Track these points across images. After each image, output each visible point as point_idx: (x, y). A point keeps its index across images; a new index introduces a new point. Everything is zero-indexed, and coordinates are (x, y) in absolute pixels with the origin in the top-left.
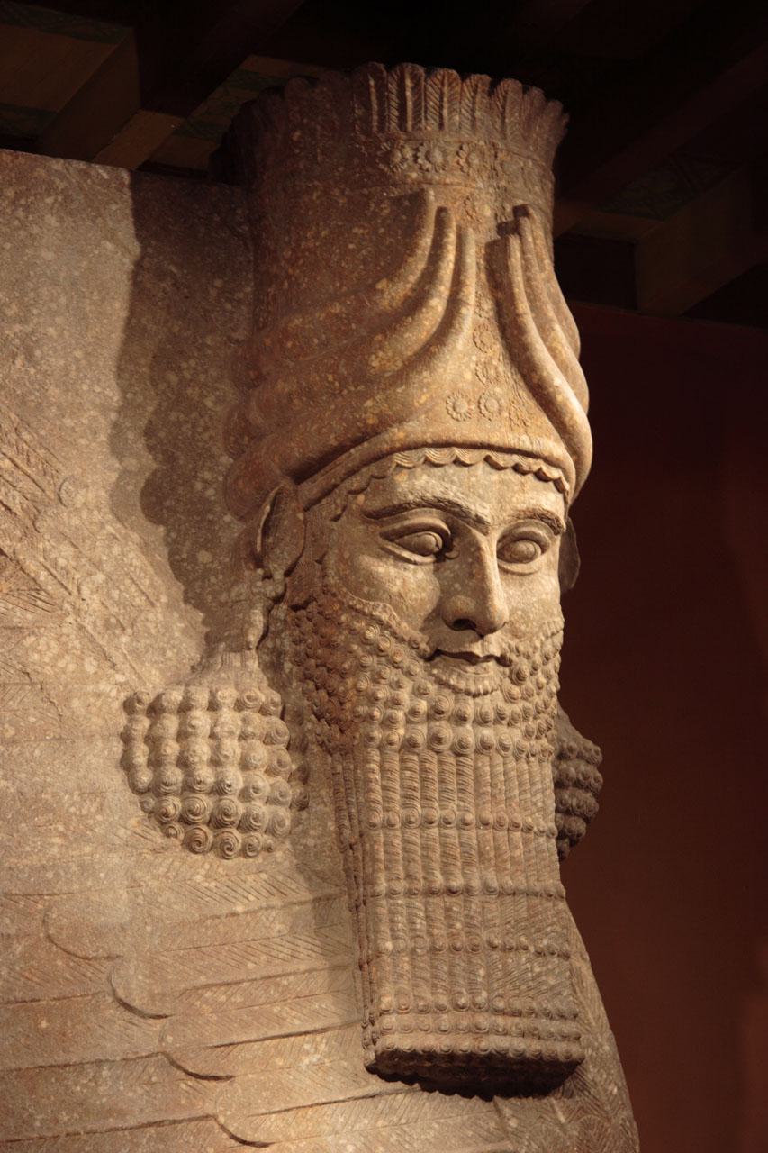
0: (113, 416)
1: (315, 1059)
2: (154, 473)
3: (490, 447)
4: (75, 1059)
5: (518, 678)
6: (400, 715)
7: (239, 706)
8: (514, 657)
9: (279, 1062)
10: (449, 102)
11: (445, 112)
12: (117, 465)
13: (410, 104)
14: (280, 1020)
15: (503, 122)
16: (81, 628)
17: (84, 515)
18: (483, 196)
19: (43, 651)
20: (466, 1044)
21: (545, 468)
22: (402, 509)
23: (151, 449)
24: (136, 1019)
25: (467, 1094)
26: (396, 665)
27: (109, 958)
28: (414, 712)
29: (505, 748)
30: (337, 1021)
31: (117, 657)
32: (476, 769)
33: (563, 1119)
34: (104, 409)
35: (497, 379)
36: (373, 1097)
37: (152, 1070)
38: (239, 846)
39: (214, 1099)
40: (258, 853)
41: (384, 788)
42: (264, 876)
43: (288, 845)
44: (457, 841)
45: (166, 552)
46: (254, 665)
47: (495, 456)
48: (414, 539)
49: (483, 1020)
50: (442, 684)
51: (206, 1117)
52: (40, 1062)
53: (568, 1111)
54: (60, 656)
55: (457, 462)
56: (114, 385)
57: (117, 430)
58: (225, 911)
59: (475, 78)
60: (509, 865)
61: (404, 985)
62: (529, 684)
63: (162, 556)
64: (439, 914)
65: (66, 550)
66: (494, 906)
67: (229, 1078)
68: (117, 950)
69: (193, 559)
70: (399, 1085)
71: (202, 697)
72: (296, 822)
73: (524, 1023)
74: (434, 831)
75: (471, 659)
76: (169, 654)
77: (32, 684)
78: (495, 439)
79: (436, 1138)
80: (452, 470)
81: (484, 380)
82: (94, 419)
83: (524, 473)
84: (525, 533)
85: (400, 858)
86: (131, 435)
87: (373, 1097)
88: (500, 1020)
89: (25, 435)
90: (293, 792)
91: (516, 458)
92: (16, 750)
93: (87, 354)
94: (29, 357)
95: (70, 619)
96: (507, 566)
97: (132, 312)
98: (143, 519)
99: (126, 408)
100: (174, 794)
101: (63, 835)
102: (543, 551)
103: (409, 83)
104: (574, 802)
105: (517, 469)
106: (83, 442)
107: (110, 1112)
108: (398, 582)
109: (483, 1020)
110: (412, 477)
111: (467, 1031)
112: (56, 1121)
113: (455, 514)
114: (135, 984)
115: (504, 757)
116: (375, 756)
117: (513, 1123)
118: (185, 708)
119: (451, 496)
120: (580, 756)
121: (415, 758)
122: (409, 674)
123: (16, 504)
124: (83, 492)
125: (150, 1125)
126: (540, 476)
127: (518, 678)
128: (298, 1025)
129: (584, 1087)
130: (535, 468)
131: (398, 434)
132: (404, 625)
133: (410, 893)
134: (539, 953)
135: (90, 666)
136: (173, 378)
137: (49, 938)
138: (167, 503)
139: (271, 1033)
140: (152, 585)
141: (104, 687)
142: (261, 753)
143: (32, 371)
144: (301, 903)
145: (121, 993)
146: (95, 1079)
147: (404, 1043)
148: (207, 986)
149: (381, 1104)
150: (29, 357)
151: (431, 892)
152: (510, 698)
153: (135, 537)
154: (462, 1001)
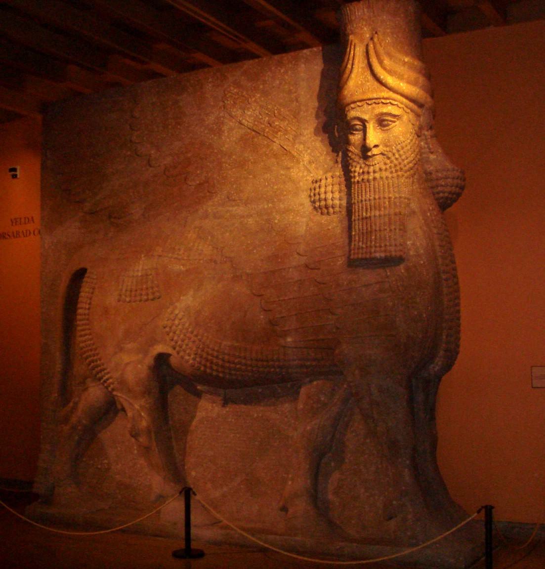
1: (341, 262)
3: (365, 100)
5: (389, 158)
6: (356, 174)
8: (386, 153)
10: (358, 10)
11: (357, 13)
16: (303, 165)
19: (294, 173)
21: (383, 101)
27: (298, 243)
31: (311, 170)
34: (313, 108)
35: (368, 81)
47: (368, 102)
54: (299, 172)
55: (358, 106)
57: (317, 112)
63: (327, 142)
65: (302, 146)
71: (324, 177)
75: (370, 157)
78: (365, 97)
80: (358, 108)
83: (379, 103)
89: (294, 121)
91: (374, 101)
94: (297, 101)
96: (385, 128)
105: (375, 103)
118: (321, 180)
119: (357, 115)
122: (358, 163)
130: (380, 102)
132: (356, 151)
135: (305, 174)
137: (285, 240)
141: (308, 178)
143: (297, 104)
145: (298, 251)
150: (297, 101)
153: (320, 139)
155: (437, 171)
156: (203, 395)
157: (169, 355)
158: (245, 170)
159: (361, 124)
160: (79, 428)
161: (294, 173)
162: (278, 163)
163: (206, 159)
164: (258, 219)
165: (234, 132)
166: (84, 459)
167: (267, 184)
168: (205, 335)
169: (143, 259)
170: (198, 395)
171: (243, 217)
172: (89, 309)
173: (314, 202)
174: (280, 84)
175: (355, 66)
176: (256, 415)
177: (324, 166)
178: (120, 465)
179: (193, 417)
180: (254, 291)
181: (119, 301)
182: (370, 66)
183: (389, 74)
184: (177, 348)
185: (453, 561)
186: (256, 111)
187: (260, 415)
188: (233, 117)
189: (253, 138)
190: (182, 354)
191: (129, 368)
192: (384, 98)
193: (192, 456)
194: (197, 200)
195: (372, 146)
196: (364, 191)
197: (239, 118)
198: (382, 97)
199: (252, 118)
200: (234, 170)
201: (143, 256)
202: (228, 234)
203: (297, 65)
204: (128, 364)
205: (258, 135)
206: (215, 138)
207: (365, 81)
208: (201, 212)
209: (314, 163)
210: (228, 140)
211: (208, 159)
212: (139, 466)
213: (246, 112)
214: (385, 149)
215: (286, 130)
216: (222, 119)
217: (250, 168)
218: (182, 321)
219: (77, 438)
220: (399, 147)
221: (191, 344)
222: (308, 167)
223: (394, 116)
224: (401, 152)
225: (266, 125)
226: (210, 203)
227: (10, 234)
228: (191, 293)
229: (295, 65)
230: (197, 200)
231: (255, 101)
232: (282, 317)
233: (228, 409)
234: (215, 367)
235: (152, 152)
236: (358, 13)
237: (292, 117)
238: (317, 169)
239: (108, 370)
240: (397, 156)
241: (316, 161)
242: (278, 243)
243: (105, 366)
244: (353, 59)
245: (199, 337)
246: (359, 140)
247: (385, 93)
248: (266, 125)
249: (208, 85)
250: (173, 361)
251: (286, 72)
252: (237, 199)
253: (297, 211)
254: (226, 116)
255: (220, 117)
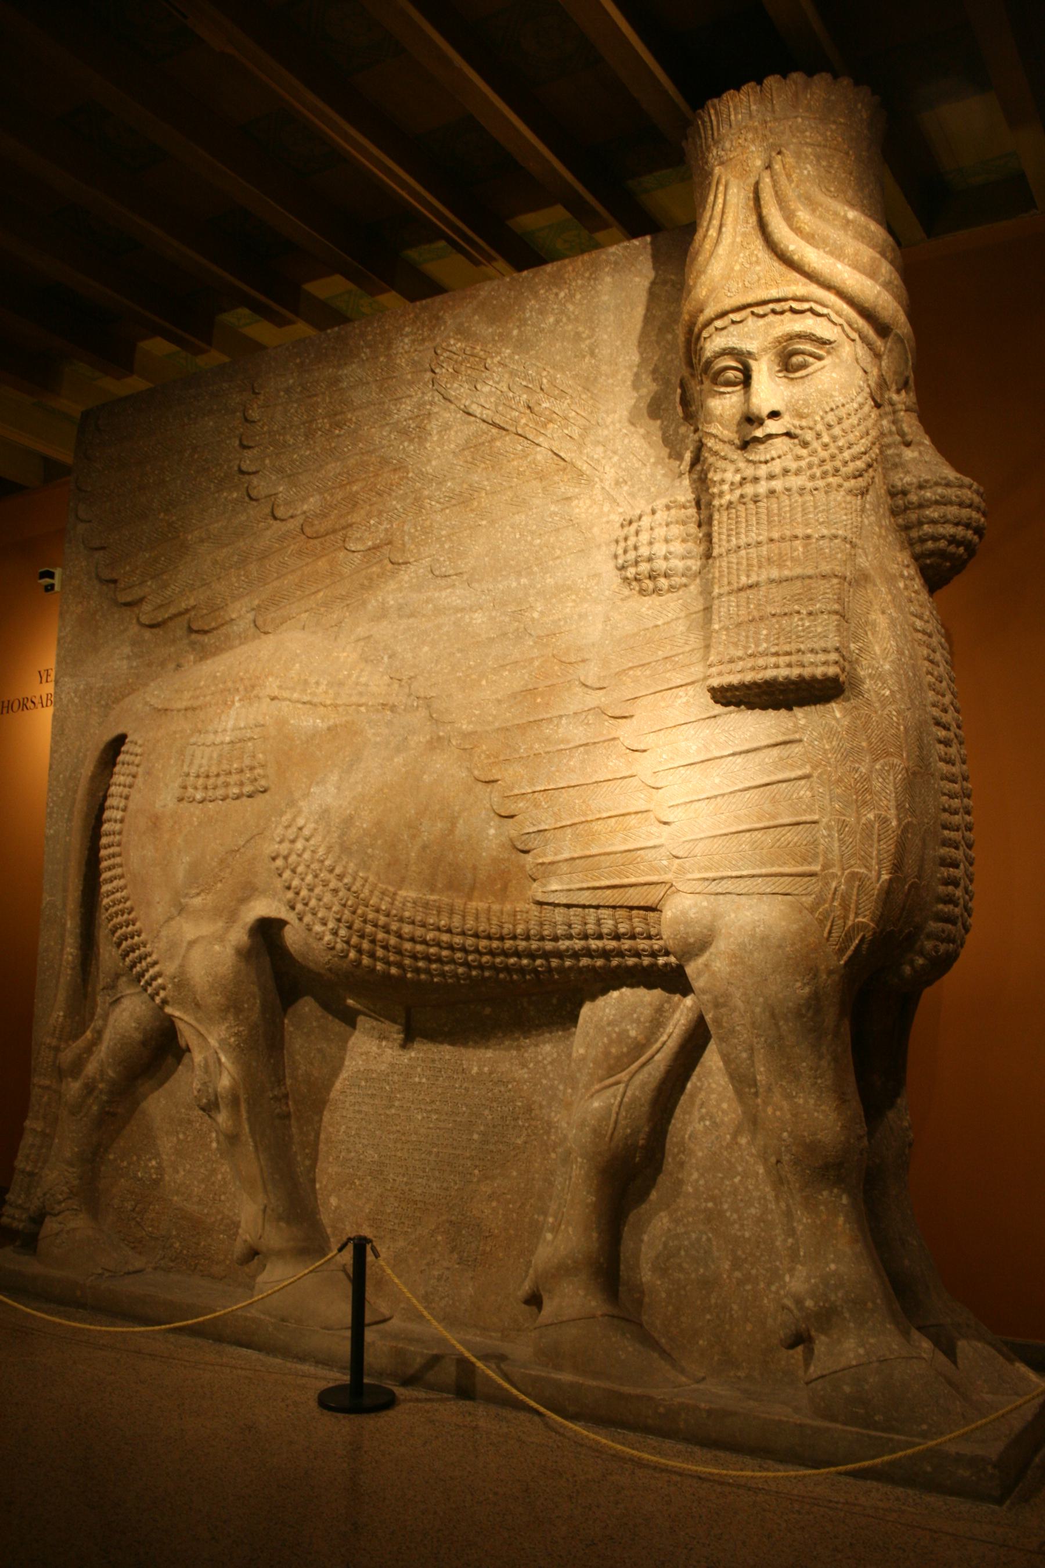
0: (635, 369)
1: (684, 700)
2: (656, 393)
4: (549, 716)
5: (805, 444)
6: (726, 487)
7: (668, 508)
8: (798, 432)
9: (663, 704)
10: (735, 109)
11: (733, 117)
12: (636, 395)
13: (715, 123)
14: (669, 680)
15: (773, 105)
16: (603, 488)
17: (611, 428)
18: (755, 155)
19: (581, 508)
20: (749, 677)
22: (709, 363)
23: (655, 380)
24: (590, 691)
25: (776, 707)
26: (725, 458)
28: (732, 484)
29: (788, 490)
30: (701, 676)
31: (620, 499)
32: (767, 508)
33: (838, 715)
34: (630, 368)
35: (757, 263)
36: (715, 717)
37: (590, 717)
38: (666, 587)
39: (625, 732)
40: (679, 589)
41: (719, 534)
42: (681, 601)
43: (698, 581)
44: (755, 555)
45: (660, 434)
46: (686, 482)
47: (756, 310)
48: (721, 379)
49: (761, 662)
50: (749, 461)
51: (614, 739)
52: (532, 719)
53: (846, 712)
54: (590, 507)
55: (733, 322)
56: (636, 351)
58: (652, 625)
59: (745, 88)
60: (789, 563)
61: (721, 648)
62: (816, 445)
63: (657, 438)
64: (743, 602)
65: (600, 449)
66: (775, 591)
67: (632, 716)
68: (587, 657)
69: (676, 432)
70: (732, 708)
72: (704, 566)
73: (794, 658)
74: (743, 553)
76: (653, 489)
77: (573, 525)
78: (750, 299)
79: (751, 736)
80: (732, 328)
81: (748, 266)
82: (625, 375)
83: (782, 313)
84: (796, 349)
85: (726, 573)
86: (644, 376)
87: (715, 717)
88: (773, 660)
89: (584, 396)
90: (699, 549)
91: (771, 306)
92: (558, 561)
93: (623, 341)
94: (592, 354)
95: (597, 486)
97: (648, 309)
98: (647, 419)
99: (644, 361)
100: (631, 566)
101: (574, 601)
102: (819, 358)
103: (712, 111)
104: (936, 515)
105: (774, 312)
106: (617, 389)
107: (562, 742)
108: (720, 408)
109: (761, 662)
110: (712, 341)
111: (753, 669)
112: (531, 748)
113: (737, 354)
114: (591, 673)
115: (789, 496)
116: (716, 516)
117: (802, 722)
118: (640, 517)
119: (731, 345)
120: (937, 484)
121: (734, 511)
123: (576, 432)
124: (611, 416)
125: (581, 746)
126: (793, 311)
127: (805, 444)
128: (679, 682)
129: (861, 693)
131: (702, 319)
132: (726, 432)
133: (730, 593)
134: (810, 614)
135: (606, 508)
136: (669, 337)
137: (554, 656)
138: (663, 407)
139: (660, 688)
140: (646, 454)
142: (676, 530)
144: (696, 613)
145: (582, 679)
146: (557, 725)
147: (715, 682)
148: (631, 668)
149: (720, 720)
150: (592, 354)
151: (740, 590)
152: (798, 458)
153: (642, 431)
154: (750, 652)
155: (921, 487)
156: (361, 1019)
157: (281, 923)
158: (472, 510)
159: (740, 366)
160: (101, 1086)
161: (581, 508)
162: (544, 489)
163: (390, 495)
164: (494, 614)
165: (453, 433)
166: (111, 1157)
167: (518, 536)
168: (361, 874)
169: (237, 704)
170: (350, 1019)
171: (462, 610)
172: (122, 821)
173: (623, 568)
174: (557, 322)
175: (727, 230)
176: (475, 1070)
177: (649, 489)
178: (182, 1173)
179: (335, 1072)
180: (476, 773)
181: (181, 800)
182: (762, 226)
183: (808, 242)
184: (299, 907)
185: (967, 1474)
186: (501, 384)
187: (486, 1069)
188: (450, 401)
189: (493, 440)
190: (308, 919)
191: (196, 953)
192: (795, 299)
193: (331, 1159)
194: (366, 582)
195: (765, 412)
196: (744, 525)
197: (463, 401)
198: (790, 296)
199: (492, 400)
200: (447, 511)
201: (237, 698)
202: (426, 649)
203: (595, 279)
204: (192, 944)
205: (504, 433)
206: (412, 447)
207: (751, 264)
208: (373, 604)
209: (626, 482)
210: (439, 450)
211: (394, 494)
212: (220, 1177)
213: (479, 387)
214: (797, 423)
215: (566, 418)
216: (428, 407)
217: (483, 505)
218: (312, 842)
219: (95, 1108)
220: (831, 418)
221: (327, 898)
222: (612, 493)
223: (823, 342)
224: (837, 431)
225: (522, 409)
226: (392, 585)
227: (36, 701)
228: (334, 778)
229: (589, 279)
230: (366, 582)
231: (500, 364)
232: (540, 831)
233: (420, 1052)
234: (380, 953)
235: (281, 489)
236: (736, 115)
237: (579, 388)
238: (633, 495)
239: (154, 957)
240: (826, 439)
241: (632, 479)
242: (536, 663)
243: (148, 949)
244: (723, 213)
245: (346, 881)
246: (732, 406)
247: (801, 287)
248: (522, 409)
249: (402, 341)
250: (293, 937)
251: (571, 296)
252: (451, 572)
253: (586, 589)
254: (436, 399)
255: (424, 403)
